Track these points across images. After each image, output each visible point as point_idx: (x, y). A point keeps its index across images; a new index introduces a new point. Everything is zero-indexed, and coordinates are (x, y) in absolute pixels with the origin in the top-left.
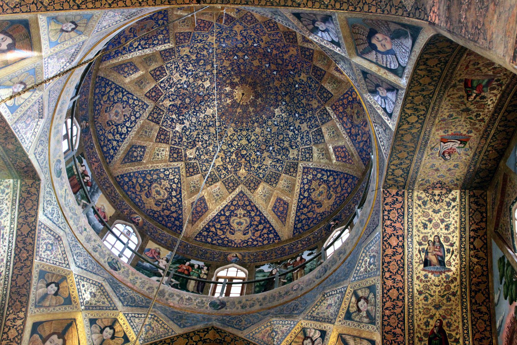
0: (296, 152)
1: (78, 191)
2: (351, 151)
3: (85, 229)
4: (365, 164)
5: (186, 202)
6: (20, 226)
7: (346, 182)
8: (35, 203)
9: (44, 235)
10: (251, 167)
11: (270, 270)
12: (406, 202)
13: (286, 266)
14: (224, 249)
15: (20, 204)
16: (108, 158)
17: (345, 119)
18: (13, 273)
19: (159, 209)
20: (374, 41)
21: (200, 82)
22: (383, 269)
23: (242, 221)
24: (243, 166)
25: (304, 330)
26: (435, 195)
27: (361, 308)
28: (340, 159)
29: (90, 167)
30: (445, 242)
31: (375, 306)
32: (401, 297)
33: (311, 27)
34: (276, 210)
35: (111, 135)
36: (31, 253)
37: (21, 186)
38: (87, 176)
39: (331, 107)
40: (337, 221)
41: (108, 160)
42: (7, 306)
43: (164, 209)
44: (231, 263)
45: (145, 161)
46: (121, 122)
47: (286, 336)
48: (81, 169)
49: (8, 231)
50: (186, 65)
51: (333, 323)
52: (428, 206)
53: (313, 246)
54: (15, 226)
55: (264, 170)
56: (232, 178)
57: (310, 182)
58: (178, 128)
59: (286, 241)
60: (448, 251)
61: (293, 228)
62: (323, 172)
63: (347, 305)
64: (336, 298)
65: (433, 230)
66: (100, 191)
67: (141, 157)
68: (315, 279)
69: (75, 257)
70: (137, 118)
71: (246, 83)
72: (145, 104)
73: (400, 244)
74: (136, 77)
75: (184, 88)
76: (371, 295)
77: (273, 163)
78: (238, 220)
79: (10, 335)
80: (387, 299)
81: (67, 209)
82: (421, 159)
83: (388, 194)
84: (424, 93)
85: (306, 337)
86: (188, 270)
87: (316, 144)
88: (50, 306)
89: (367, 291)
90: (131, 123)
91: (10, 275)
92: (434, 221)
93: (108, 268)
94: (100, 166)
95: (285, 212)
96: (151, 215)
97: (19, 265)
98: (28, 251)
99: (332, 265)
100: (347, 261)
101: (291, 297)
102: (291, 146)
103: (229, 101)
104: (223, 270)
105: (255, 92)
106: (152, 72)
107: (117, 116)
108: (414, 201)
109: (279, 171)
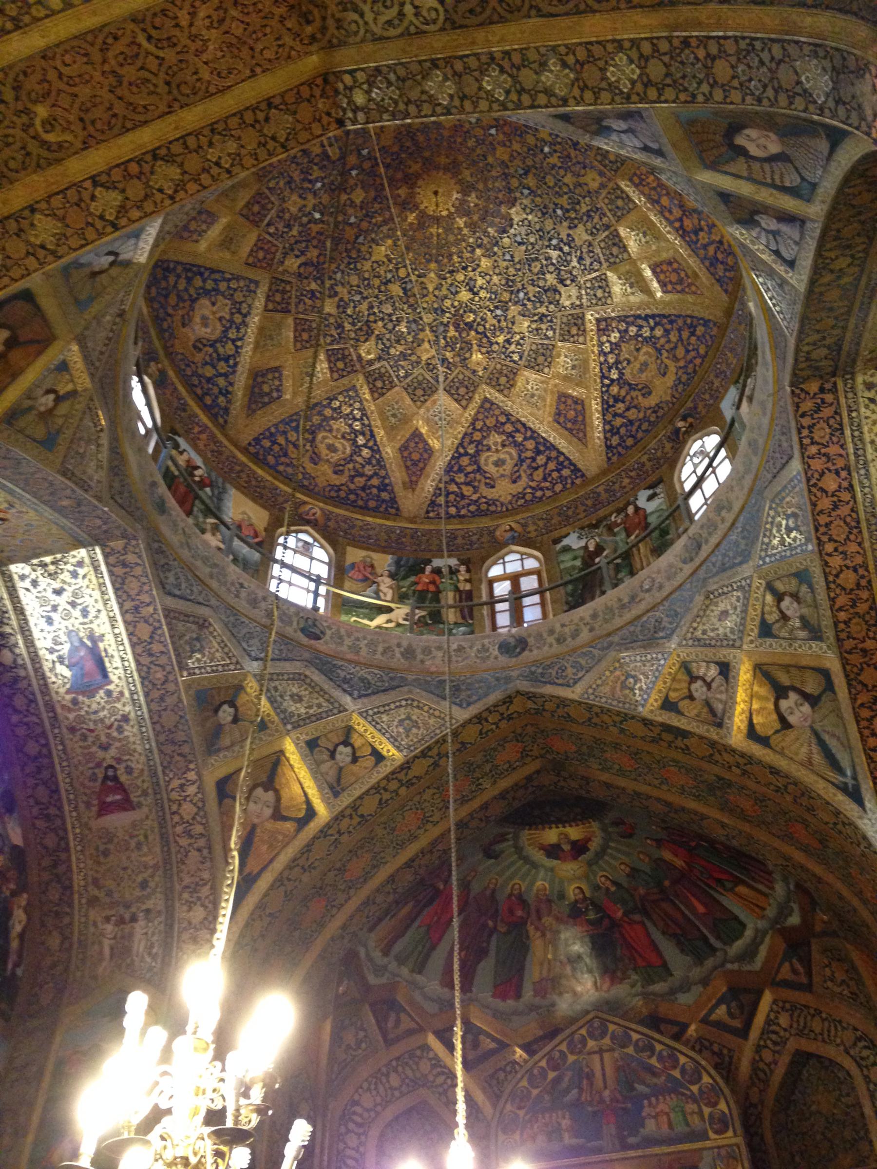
0: (574, 292)
1: (193, 505)
2: (689, 267)
3: (242, 586)
4: (726, 291)
5: (389, 450)
6: (131, 629)
7: (693, 334)
8: (144, 580)
9: (180, 626)
10: (492, 344)
11: (582, 543)
12: (843, 401)
13: (610, 529)
14: (485, 523)
15: (116, 590)
16: (218, 413)
17: (665, 201)
18: (150, 711)
19: (344, 479)
20: (740, 140)
21: (344, 197)
22: (818, 538)
23: (502, 456)
24: (475, 347)
25: (685, 666)
27: (789, 613)
28: (670, 287)
29: (195, 447)
31: (816, 607)
32: (863, 582)
33: (594, 127)
34: (562, 420)
35: (208, 367)
36: (168, 668)
37: (106, 556)
38: (198, 468)
39: (631, 180)
40: (690, 420)
41: (221, 420)
42: (160, 769)
43: (353, 477)
44: (506, 544)
45: (288, 397)
46: (218, 333)
47: (654, 683)
48: (181, 460)
50: (306, 172)
51: (740, 647)
53: (653, 478)
54: (121, 628)
55: (518, 344)
56: (461, 377)
57: (615, 346)
58: (329, 307)
59: (597, 477)
61: (604, 448)
62: (640, 322)
63: (759, 612)
64: (734, 599)
66: (228, 486)
67: (278, 390)
68: (681, 565)
69: (244, 645)
70: (245, 316)
71: (437, 168)
72: (251, 281)
73: (845, 484)
74: (217, 232)
75: (316, 222)
76: (804, 589)
77: (534, 326)
78: (495, 458)
79: (184, 814)
80: (838, 591)
81: (199, 563)
82: (864, 320)
83: (803, 395)
84: (862, 218)
85: (693, 679)
86: (433, 582)
87: (612, 266)
88: (233, 744)
89: (794, 582)
90: (238, 329)
91: (146, 716)
93: (305, 640)
94: (212, 438)
95: (580, 418)
96: (334, 496)
97: (156, 694)
98: (163, 667)
99: (710, 534)
100: (739, 525)
101: (643, 607)
102: (562, 281)
103: (412, 217)
104: (495, 563)
105: (460, 182)
106: (244, 212)
107: (206, 325)
108: (860, 394)
109: (548, 338)
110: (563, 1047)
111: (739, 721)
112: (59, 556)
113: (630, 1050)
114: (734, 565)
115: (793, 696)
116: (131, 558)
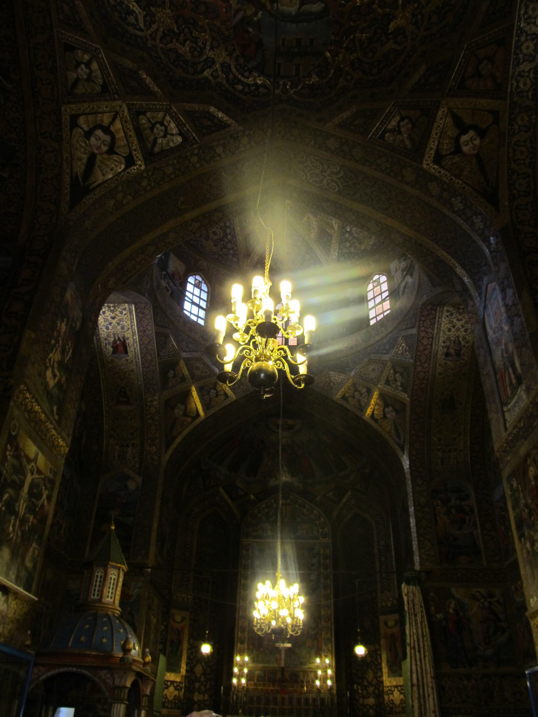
6: (141, 338)
12: (438, 314)
18: (143, 370)
26: (460, 309)
27: (398, 379)
30: (462, 340)
32: (426, 378)
37: (136, 309)
49: (132, 341)
52: (454, 316)
54: (137, 337)
60: (464, 346)
65: (455, 332)
85: (356, 390)
91: (141, 372)
92: (457, 327)
110: (272, 501)
111: (369, 411)
112: (116, 305)
113: (297, 506)
114: (382, 353)
115: (391, 408)
116: (146, 311)
